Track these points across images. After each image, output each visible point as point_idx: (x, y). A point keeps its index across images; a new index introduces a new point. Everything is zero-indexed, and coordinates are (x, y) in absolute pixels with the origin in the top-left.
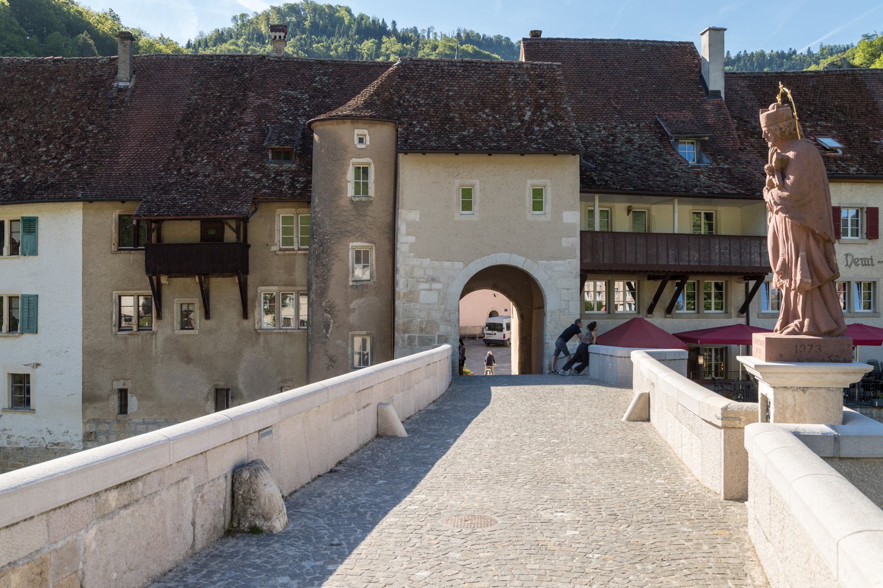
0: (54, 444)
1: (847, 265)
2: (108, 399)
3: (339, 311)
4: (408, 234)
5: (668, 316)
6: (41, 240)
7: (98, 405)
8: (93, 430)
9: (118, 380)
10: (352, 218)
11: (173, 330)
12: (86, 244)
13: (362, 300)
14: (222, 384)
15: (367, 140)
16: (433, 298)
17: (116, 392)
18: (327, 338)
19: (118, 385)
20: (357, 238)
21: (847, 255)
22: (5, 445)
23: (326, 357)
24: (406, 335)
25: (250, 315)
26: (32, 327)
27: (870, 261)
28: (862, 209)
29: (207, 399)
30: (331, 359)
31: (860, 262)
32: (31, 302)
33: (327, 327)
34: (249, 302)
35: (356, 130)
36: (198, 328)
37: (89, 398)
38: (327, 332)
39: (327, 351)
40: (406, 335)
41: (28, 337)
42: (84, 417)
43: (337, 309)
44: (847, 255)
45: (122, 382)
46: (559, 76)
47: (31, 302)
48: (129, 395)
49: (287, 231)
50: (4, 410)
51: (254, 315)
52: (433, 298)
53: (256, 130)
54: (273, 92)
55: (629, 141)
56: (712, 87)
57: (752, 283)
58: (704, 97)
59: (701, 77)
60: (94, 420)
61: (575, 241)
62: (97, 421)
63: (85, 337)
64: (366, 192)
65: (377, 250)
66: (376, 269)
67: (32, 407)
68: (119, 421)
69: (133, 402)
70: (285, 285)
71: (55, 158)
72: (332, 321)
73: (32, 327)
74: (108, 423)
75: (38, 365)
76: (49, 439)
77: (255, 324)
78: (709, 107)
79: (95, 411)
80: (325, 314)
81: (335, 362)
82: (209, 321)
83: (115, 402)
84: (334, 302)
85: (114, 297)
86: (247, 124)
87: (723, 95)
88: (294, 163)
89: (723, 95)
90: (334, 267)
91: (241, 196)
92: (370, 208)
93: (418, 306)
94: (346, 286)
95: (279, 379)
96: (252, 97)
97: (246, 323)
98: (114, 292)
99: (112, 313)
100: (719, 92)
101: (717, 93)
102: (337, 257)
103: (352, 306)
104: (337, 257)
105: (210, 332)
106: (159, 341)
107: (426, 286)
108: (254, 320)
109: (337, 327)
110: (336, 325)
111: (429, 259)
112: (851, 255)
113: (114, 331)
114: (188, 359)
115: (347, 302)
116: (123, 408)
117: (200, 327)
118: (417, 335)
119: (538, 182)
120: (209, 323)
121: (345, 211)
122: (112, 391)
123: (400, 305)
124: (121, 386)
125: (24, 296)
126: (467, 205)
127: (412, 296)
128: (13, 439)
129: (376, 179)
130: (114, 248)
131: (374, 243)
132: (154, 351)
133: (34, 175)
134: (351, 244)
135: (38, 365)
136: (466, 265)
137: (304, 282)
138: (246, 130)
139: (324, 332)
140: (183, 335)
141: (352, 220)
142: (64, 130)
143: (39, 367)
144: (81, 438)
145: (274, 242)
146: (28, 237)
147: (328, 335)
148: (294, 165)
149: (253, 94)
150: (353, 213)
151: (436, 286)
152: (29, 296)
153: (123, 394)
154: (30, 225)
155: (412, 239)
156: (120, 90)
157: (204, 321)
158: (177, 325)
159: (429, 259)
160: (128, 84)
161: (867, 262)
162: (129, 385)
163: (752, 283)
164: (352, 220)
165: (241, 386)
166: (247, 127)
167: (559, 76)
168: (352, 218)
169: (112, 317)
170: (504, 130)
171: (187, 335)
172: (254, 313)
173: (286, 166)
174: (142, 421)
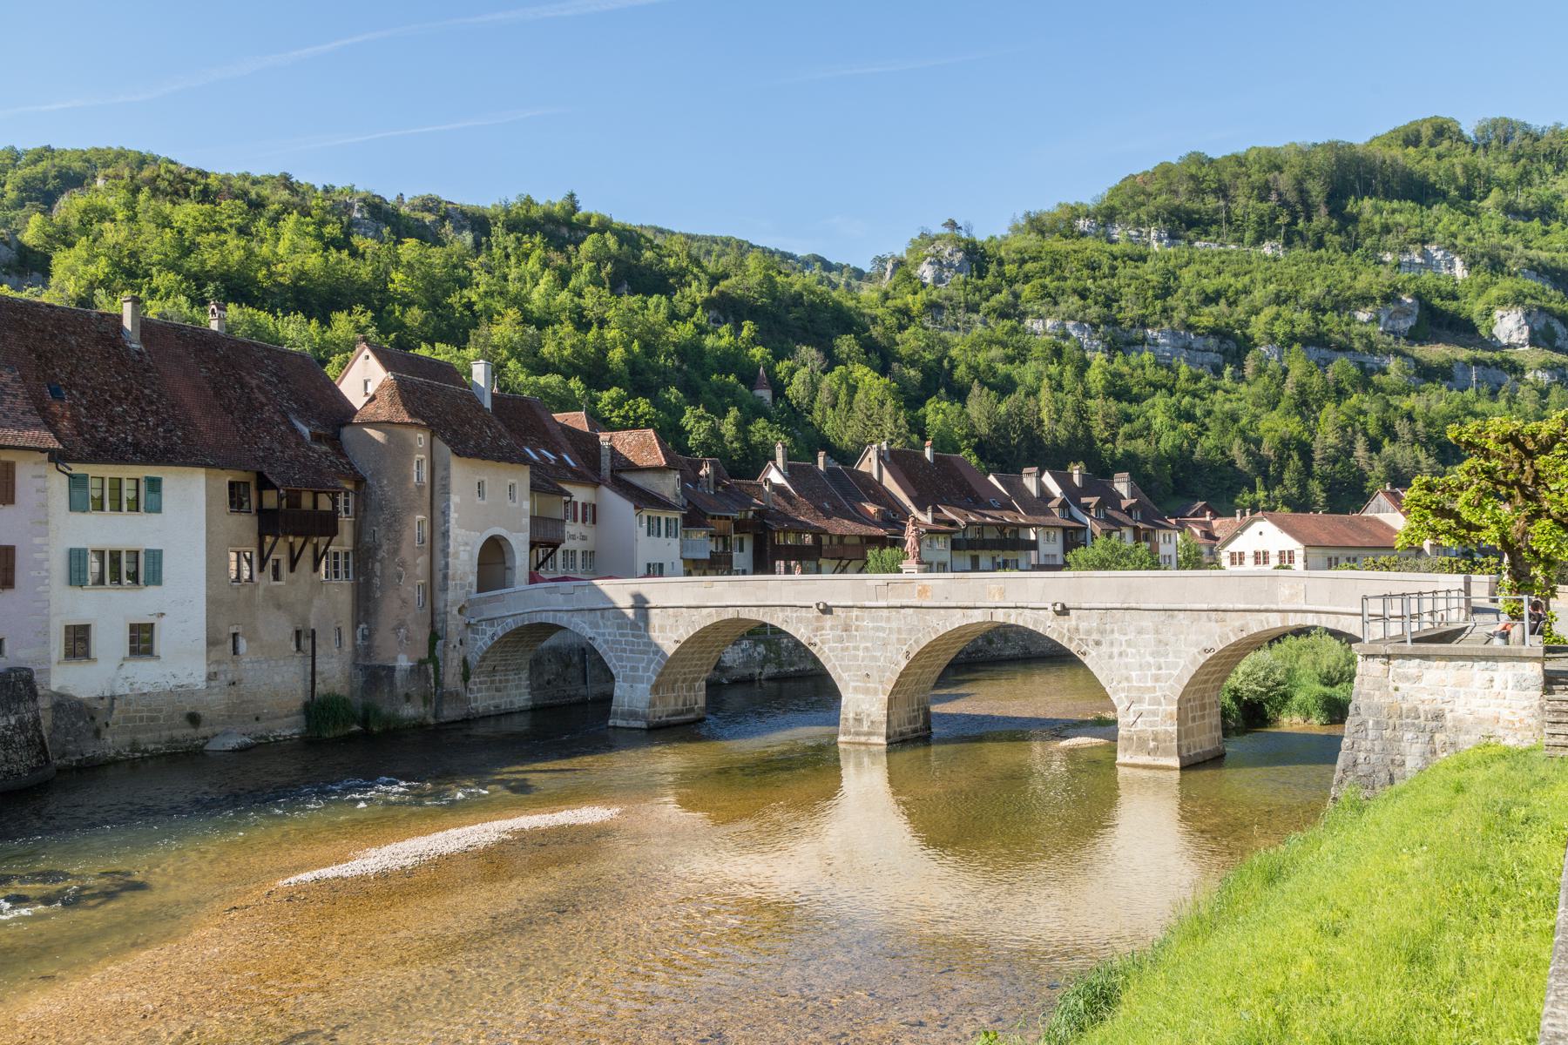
12: (209, 504)
14: (300, 626)
19: (233, 630)
22: (128, 692)
26: (155, 578)
30: (404, 601)
32: (155, 557)
33: (400, 577)
37: (212, 642)
41: (152, 589)
42: (208, 659)
47: (155, 557)
49: (346, 502)
50: (124, 659)
57: (550, 550)
61: (526, 521)
62: (218, 662)
63: (208, 588)
67: (156, 653)
69: (243, 644)
73: (155, 578)
75: (162, 614)
76: (173, 682)
97: (315, 576)
106: (261, 591)
114: (279, 607)
115: (415, 559)
116: (235, 651)
120: (293, 575)
125: (147, 552)
126: (481, 493)
128: (136, 686)
135: (162, 614)
136: (481, 533)
144: (204, 678)
146: (152, 496)
151: (468, 548)
152: (154, 551)
153: (235, 635)
154: (155, 485)
155: (456, 515)
158: (271, 577)
162: (240, 630)
163: (550, 550)
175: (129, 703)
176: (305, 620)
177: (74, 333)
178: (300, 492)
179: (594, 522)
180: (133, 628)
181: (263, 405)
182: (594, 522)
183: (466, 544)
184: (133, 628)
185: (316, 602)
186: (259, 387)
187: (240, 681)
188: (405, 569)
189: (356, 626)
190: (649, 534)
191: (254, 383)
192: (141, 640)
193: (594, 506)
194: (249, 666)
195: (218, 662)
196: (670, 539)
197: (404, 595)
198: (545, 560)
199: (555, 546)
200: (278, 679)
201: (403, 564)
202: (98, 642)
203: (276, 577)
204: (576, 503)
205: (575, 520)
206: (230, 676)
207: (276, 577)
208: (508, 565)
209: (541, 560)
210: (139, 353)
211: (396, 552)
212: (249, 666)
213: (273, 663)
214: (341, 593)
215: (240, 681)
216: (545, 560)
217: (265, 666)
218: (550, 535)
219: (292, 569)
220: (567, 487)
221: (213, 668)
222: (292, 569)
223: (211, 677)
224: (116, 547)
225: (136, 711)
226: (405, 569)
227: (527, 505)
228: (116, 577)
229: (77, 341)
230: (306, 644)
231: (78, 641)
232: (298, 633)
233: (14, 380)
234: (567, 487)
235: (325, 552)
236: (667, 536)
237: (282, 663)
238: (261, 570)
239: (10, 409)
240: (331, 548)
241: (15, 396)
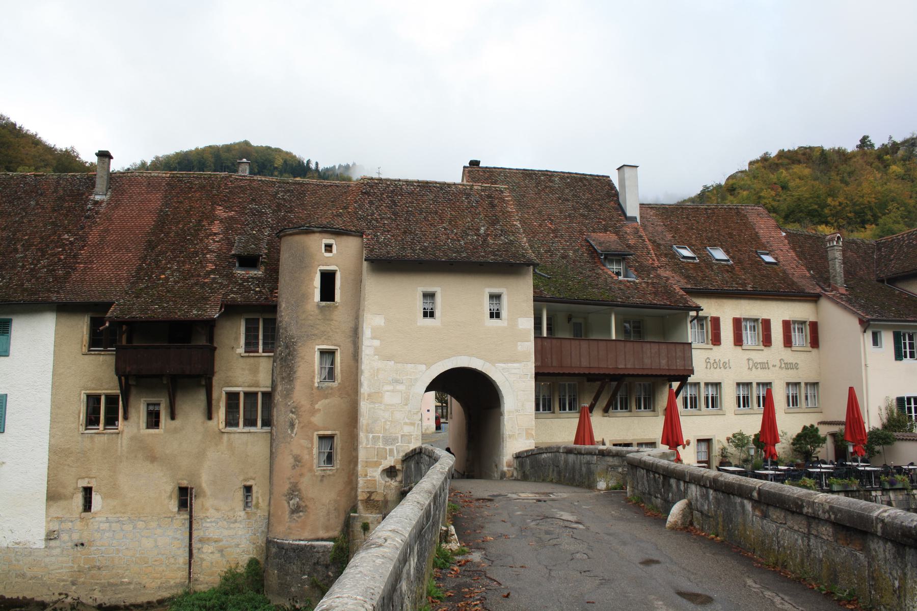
0: (16, 543)
1: (749, 368)
2: (72, 498)
3: (304, 412)
4: (373, 338)
5: (606, 414)
6: (13, 342)
7: (63, 503)
8: (56, 528)
9: (83, 478)
10: (318, 322)
11: (139, 429)
13: (327, 401)
14: (185, 483)
15: (334, 248)
16: (396, 400)
17: (81, 489)
18: (292, 437)
19: (84, 483)
20: (323, 341)
21: (749, 360)
23: (291, 456)
24: (371, 436)
25: (214, 415)
27: (766, 365)
28: (756, 320)
29: (170, 497)
31: (759, 366)
33: (292, 425)
34: (214, 402)
35: (324, 240)
36: (163, 427)
37: (53, 497)
38: (292, 431)
39: (291, 451)
40: (371, 436)
42: (47, 515)
43: (303, 409)
44: (749, 360)
45: (87, 480)
46: (506, 197)
48: (93, 494)
51: (218, 415)
52: (396, 400)
53: (223, 240)
54: (239, 206)
55: (564, 257)
56: (629, 214)
58: (623, 221)
59: (619, 205)
60: (57, 518)
62: (60, 520)
63: (52, 436)
64: (332, 298)
65: (341, 353)
66: (341, 371)
68: (82, 519)
69: (96, 500)
70: (249, 386)
71: (31, 264)
72: (297, 421)
74: (72, 521)
77: (219, 423)
78: (628, 231)
79: (58, 510)
80: (291, 414)
81: (299, 462)
82: (173, 422)
83: (79, 499)
84: (300, 402)
85: (82, 397)
86: (215, 234)
87: (638, 220)
88: (259, 270)
89: (638, 220)
90: (300, 369)
91: (210, 300)
92: (336, 313)
93: (382, 407)
94: (312, 388)
95: (241, 478)
96: (220, 210)
97: (210, 423)
98: (83, 392)
99: (79, 413)
100: (635, 218)
101: (634, 219)
102: (303, 359)
103: (317, 406)
104: (303, 359)
105: (176, 431)
107: (390, 388)
108: (219, 420)
109: (302, 427)
110: (302, 425)
111: (393, 362)
112: (752, 360)
113: (81, 430)
114: (153, 458)
116: (87, 506)
117: (165, 426)
118: (381, 435)
119: (495, 290)
121: (311, 316)
122: (77, 488)
123: (364, 406)
124: (85, 485)
127: (375, 397)
129: (341, 285)
130: (85, 350)
131: (339, 346)
132: (119, 449)
133: (10, 279)
134: (317, 347)
137: (269, 383)
138: (213, 240)
139: (289, 432)
140: (149, 435)
141: (318, 324)
142: (42, 238)
143: (4, 465)
144: (43, 537)
145: (239, 343)
147: (293, 435)
148: (261, 273)
149: (221, 208)
150: (320, 317)
151: (400, 387)
153: (88, 491)
155: (377, 343)
156: (96, 203)
157: (169, 421)
158: (143, 423)
159: (393, 362)
160: (104, 197)
161: (764, 366)
162: (93, 484)
164: (318, 324)
165: (204, 485)
166: (215, 237)
167: (506, 197)
168: (318, 322)
169: (79, 417)
170: (462, 243)
171: (152, 435)
172: (218, 413)
173: (253, 273)
174: (105, 519)
178: (210, 326)
179: (815, 342)
183: (397, 381)
187: (91, 543)
188: (298, 416)
193: (814, 326)
194: (105, 526)
195: (60, 520)
200: (148, 543)
201: (295, 410)
206: (76, 537)
207: (153, 421)
211: (288, 394)
212: (105, 526)
213: (141, 524)
215: (91, 543)
217: (128, 527)
219: (173, 417)
221: (55, 526)
222: (173, 417)
223: (51, 536)
226: (298, 416)
227: (528, 323)
237: (154, 524)
238: (126, 418)
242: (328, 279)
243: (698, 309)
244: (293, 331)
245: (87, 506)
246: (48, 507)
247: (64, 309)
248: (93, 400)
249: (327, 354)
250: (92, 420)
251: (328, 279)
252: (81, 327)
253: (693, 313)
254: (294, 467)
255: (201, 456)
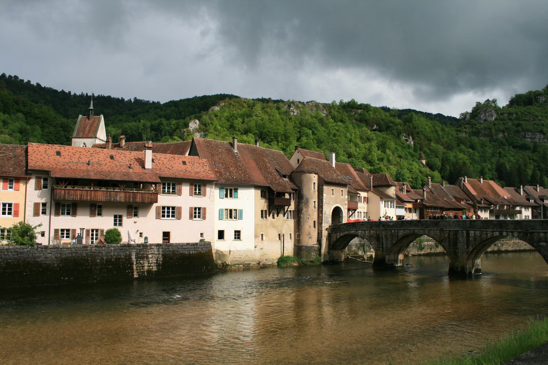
14: (280, 233)
19: (262, 233)
26: (241, 218)
32: (241, 211)
33: (309, 218)
37: (256, 236)
57: (353, 211)
61: (347, 202)
69: (264, 237)
106: (269, 222)
114: (274, 227)
116: (262, 239)
153: (262, 235)
162: (263, 233)
175: (234, 253)
176: (281, 231)
177: (220, 148)
180: (235, 231)
181: (270, 167)
182: (367, 203)
184: (235, 231)
185: (285, 226)
186: (268, 162)
189: (295, 234)
190: (385, 207)
191: (267, 161)
192: (238, 235)
196: (392, 208)
197: (310, 224)
198: (352, 215)
199: (355, 210)
201: (309, 215)
202: (226, 235)
203: (273, 218)
204: (361, 197)
205: (361, 202)
206: (261, 247)
207: (273, 218)
208: (341, 215)
209: (350, 215)
210: (237, 153)
214: (291, 223)
216: (352, 215)
218: (353, 206)
219: (278, 216)
220: (359, 192)
222: (278, 216)
224: (231, 208)
225: (236, 255)
226: (310, 216)
228: (231, 217)
229: (221, 150)
230: (282, 238)
231: (221, 235)
232: (279, 235)
233: (206, 162)
234: (359, 192)
235: (287, 210)
236: (391, 207)
239: (205, 170)
240: (288, 209)
241: (206, 166)
242: (314, 183)
243: (360, 194)
244: (308, 196)
245: (262, 239)
246: (255, 239)
247: (256, 187)
248: (262, 211)
249: (315, 202)
250: (262, 217)
251: (314, 183)
252: (259, 192)
253: (358, 195)
254: (309, 228)
255: (282, 226)
